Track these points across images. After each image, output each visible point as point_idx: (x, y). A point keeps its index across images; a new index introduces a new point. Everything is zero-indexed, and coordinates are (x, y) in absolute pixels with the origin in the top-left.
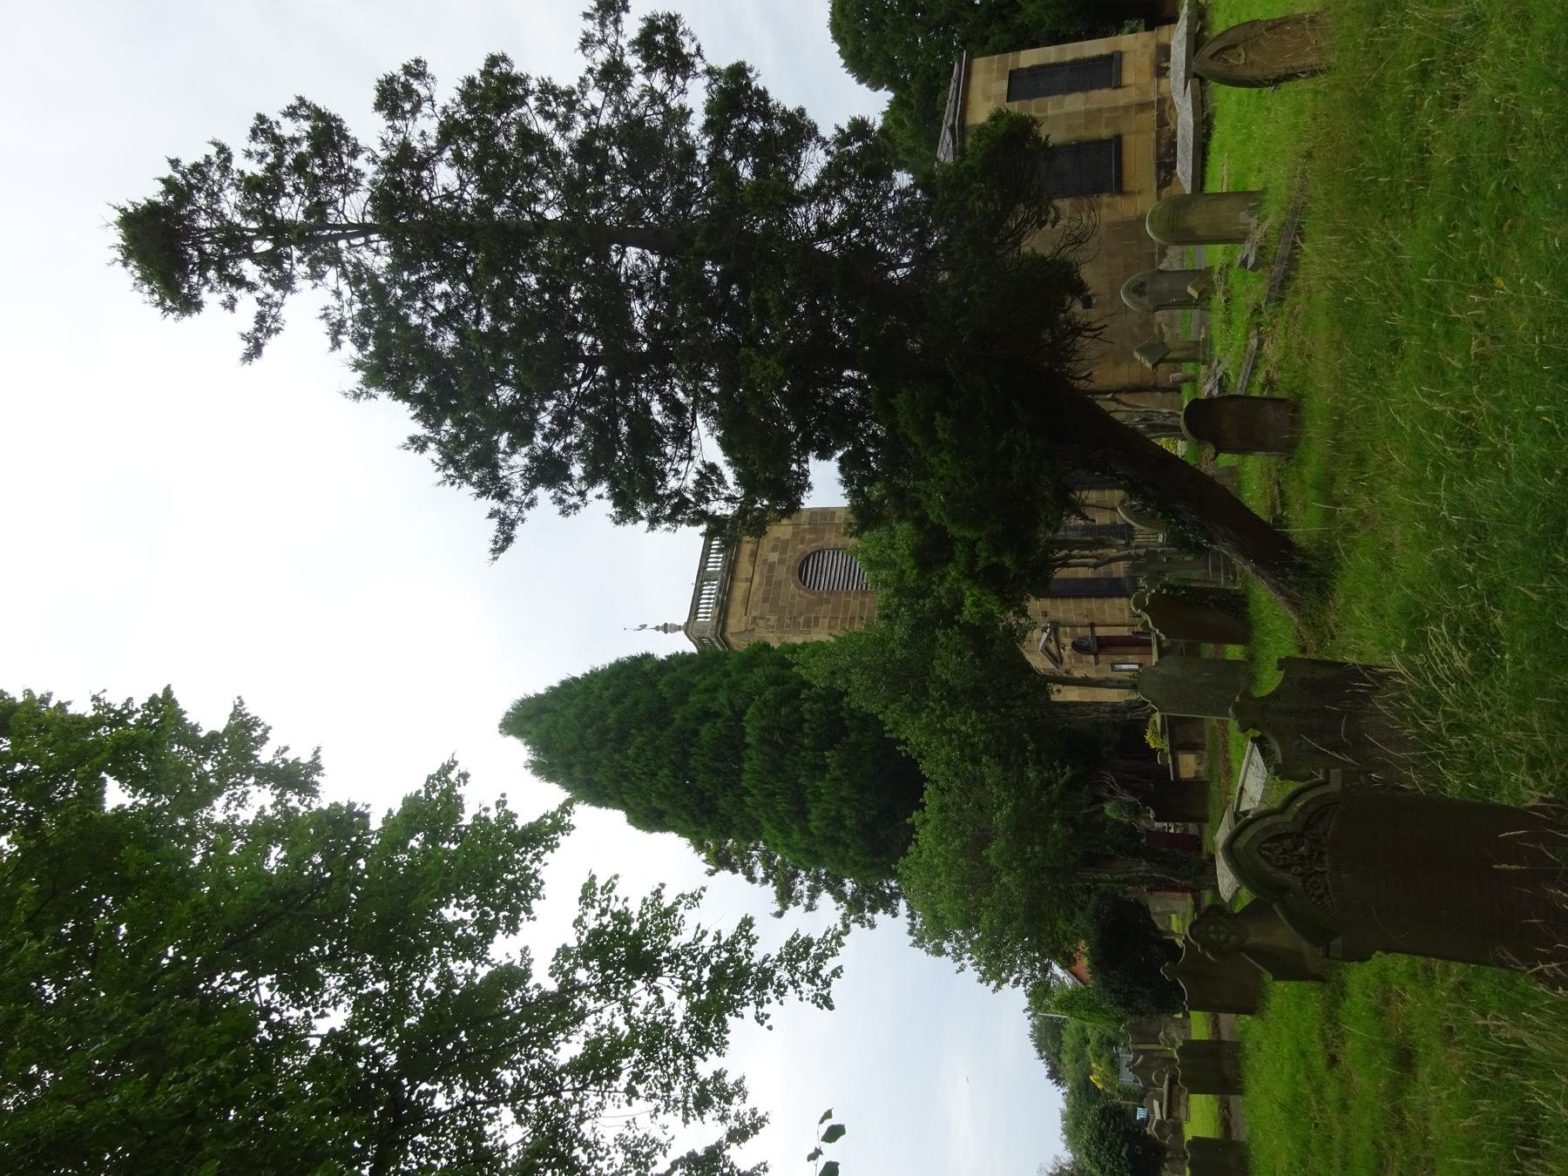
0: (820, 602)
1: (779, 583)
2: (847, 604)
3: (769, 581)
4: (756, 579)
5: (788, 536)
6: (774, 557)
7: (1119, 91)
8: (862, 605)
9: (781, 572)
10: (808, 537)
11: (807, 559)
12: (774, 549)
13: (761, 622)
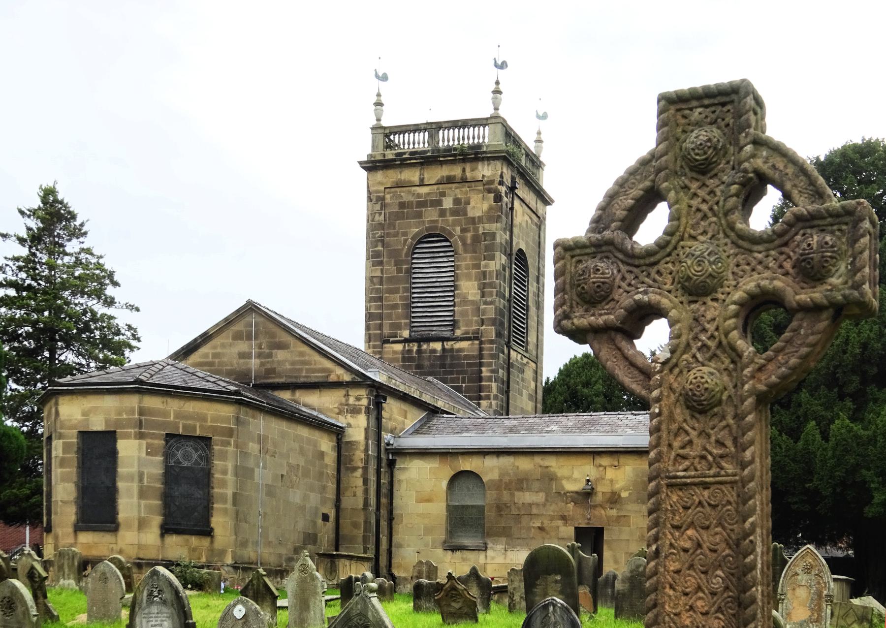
0: (398, 263)
1: (419, 215)
2: (394, 291)
3: (422, 204)
4: (424, 190)
5: (470, 214)
6: (448, 203)
7: (70, 530)
8: (395, 307)
9: (431, 215)
10: (469, 235)
11: (447, 240)
12: (457, 201)
13: (378, 207)
